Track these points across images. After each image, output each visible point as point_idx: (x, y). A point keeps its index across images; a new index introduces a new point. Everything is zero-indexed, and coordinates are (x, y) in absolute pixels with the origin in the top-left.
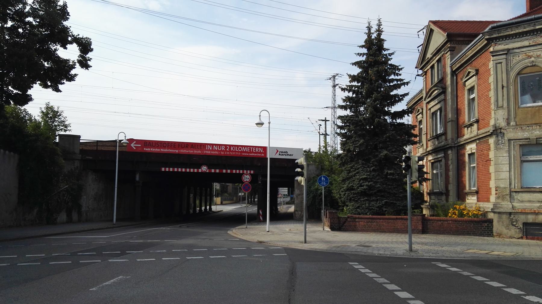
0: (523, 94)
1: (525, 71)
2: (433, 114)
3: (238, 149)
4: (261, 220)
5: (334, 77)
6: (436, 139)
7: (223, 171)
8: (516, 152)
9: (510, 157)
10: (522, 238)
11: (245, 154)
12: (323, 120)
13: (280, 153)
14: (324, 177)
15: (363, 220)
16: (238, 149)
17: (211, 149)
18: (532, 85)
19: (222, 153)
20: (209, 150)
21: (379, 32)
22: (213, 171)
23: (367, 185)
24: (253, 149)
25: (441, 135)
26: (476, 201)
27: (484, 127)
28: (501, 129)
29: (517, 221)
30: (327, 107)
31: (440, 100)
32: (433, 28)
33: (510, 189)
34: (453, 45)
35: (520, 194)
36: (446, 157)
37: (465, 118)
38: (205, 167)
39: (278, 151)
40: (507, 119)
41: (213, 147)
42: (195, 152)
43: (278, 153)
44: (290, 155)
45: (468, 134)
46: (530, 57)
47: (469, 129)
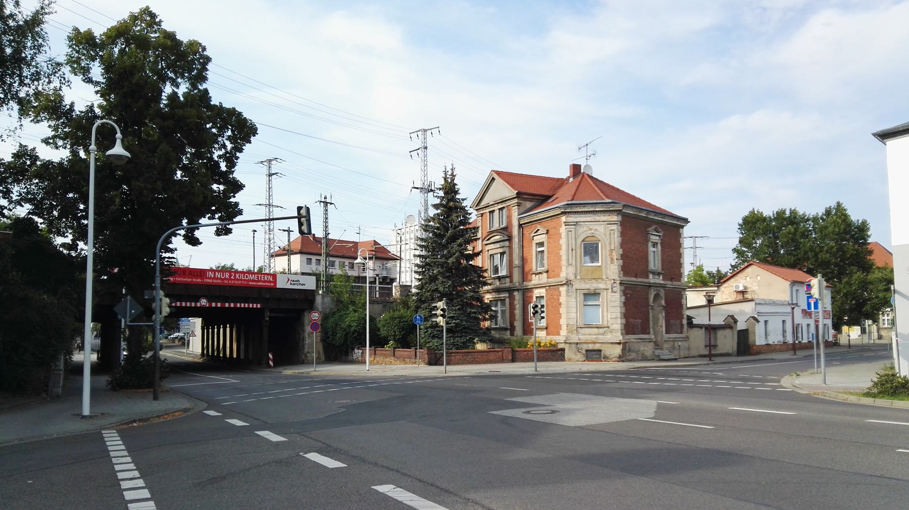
0: (585, 256)
1: (587, 239)
2: (491, 255)
3: (244, 277)
4: (271, 365)
5: (270, 161)
6: (497, 280)
7: (221, 305)
8: (581, 298)
9: (576, 302)
10: (585, 361)
11: (252, 283)
12: (284, 231)
13: (292, 282)
14: (419, 316)
15: (459, 354)
16: (244, 277)
17: (213, 276)
18: (591, 250)
19: (226, 282)
20: (211, 278)
21: (453, 176)
22: (214, 305)
23: (454, 323)
24: (261, 277)
25: (504, 277)
26: (545, 335)
27: (554, 277)
28: (570, 281)
29: (581, 349)
30: (260, 205)
31: (503, 245)
32: (494, 177)
33: (577, 326)
34: (520, 202)
35: (583, 329)
36: (512, 298)
37: (533, 265)
38: (205, 301)
39: (289, 280)
40: (575, 274)
41: (215, 275)
42: (194, 280)
43: (290, 281)
44: (303, 285)
45: (535, 280)
46: (591, 229)
47: (537, 276)
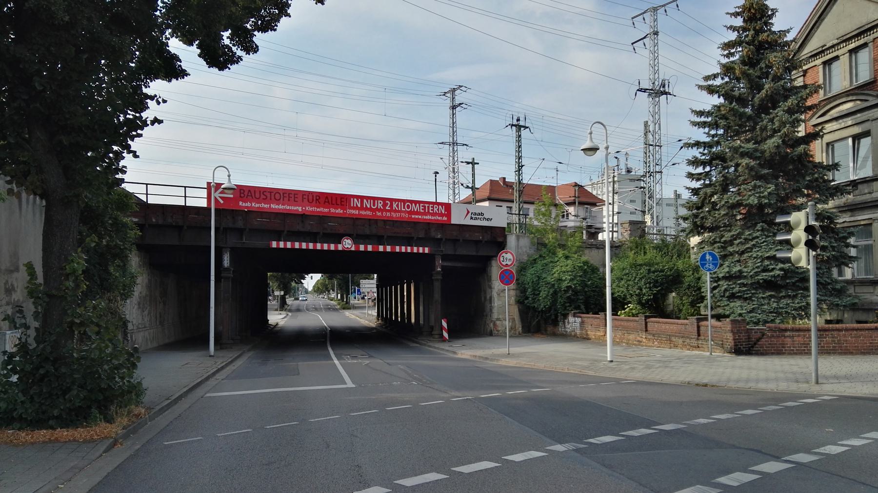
2: (828, 144)
3: (404, 208)
5: (454, 90)
7: (373, 248)
11: (417, 217)
12: (468, 163)
13: (473, 216)
16: (404, 208)
17: (359, 206)
19: (379, 214)
20: (356, 208)
22: (362, 248)
23: (781, 269)
30: (442, 143)
39: (468, 212)
41: (362, 203)
42: (333, 210)
43: (470, 213)
44: (488, 220)
